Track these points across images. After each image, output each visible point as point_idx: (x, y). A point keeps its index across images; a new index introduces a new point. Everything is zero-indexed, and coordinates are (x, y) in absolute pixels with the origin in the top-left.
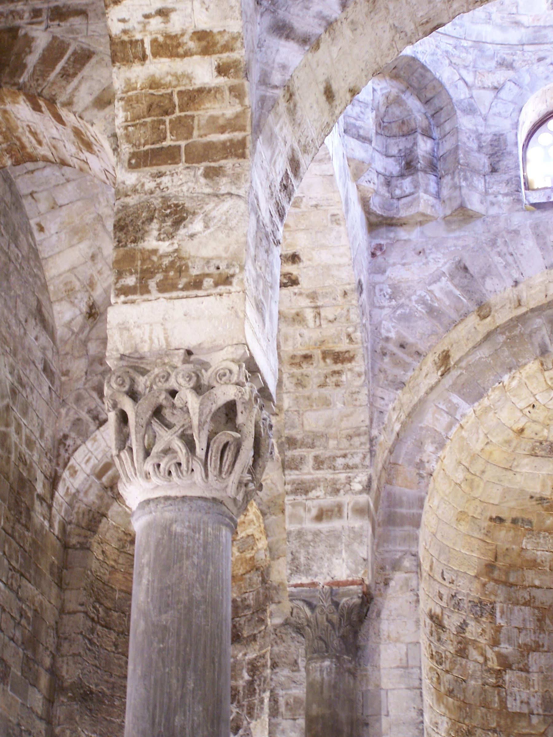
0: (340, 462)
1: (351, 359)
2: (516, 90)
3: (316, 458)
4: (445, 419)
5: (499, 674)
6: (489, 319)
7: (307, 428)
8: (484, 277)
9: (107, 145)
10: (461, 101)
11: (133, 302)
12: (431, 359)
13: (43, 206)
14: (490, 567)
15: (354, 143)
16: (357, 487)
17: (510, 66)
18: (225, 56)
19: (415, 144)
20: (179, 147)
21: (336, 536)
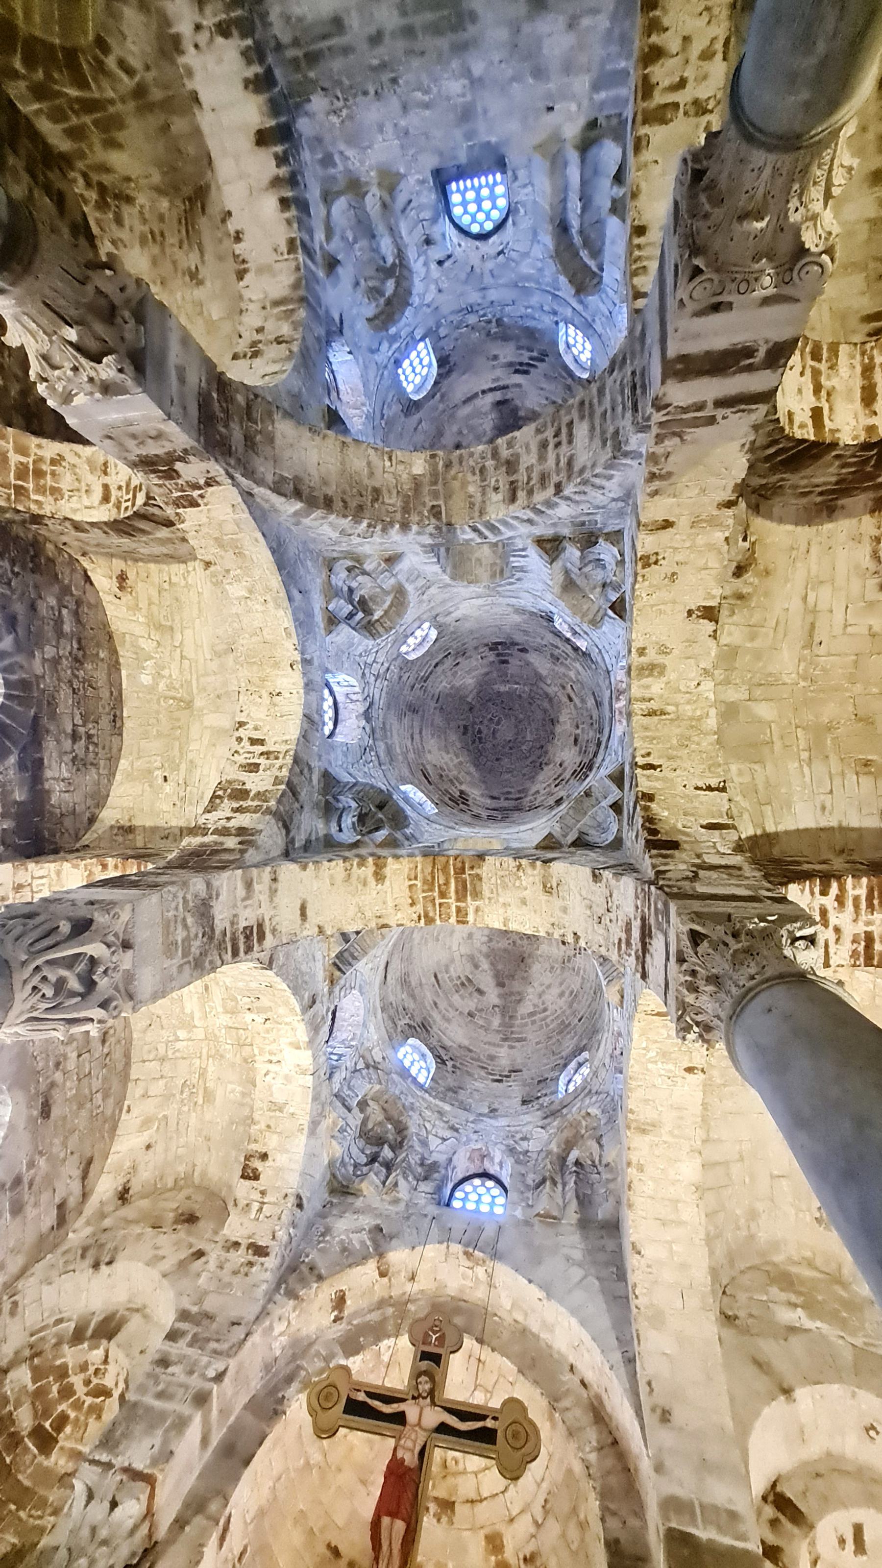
1: (267, 1255)
6: (386, 1279)
8: (391, 1238)
13: (139, 1092)
16: (211, 1373)
17: (457, 1130)
21: (162, 1416)
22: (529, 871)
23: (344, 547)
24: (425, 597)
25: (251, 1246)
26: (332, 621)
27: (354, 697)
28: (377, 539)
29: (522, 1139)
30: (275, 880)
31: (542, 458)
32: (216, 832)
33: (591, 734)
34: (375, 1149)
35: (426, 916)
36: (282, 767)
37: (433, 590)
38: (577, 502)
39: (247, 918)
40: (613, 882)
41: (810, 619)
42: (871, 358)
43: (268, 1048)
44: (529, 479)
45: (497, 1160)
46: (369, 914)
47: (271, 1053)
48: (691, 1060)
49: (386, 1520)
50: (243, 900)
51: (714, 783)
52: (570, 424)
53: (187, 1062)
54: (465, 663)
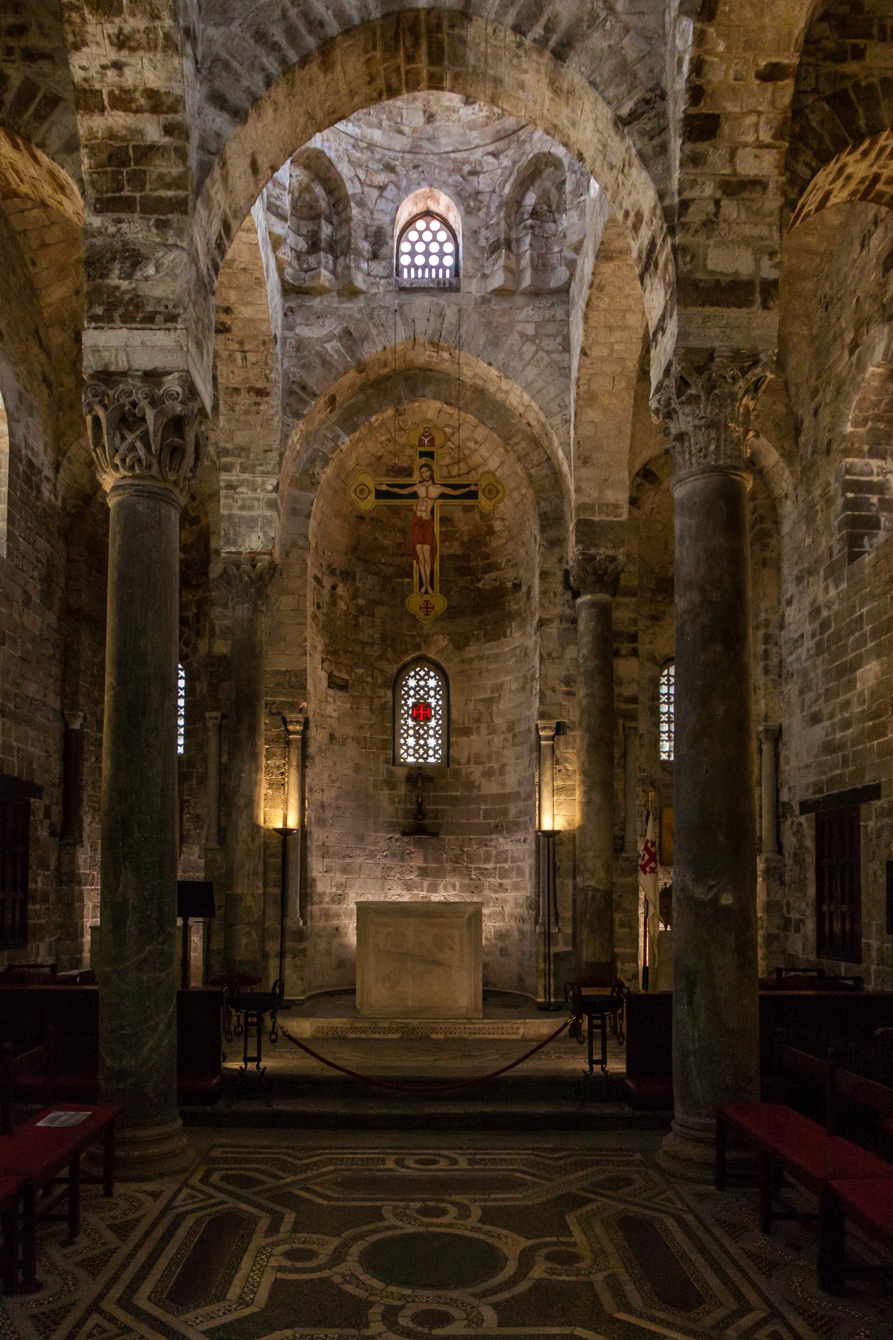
0: (259, 468)
1: (268, 394)
2: (395, 191)
3: (242, 464)
4: (331, 445)
5: (356, 617)
7: (236, 442)
9: (76, 188)
10: (354, 195)
11: (102, 328)
12: (322, 401)
14: (355, 549)
15: (273, 219)
16: (270, 488)
19: (320, 227)
20: (135, 198)
25: (250, 389)
34: (311, 226)
49: (419, 547)
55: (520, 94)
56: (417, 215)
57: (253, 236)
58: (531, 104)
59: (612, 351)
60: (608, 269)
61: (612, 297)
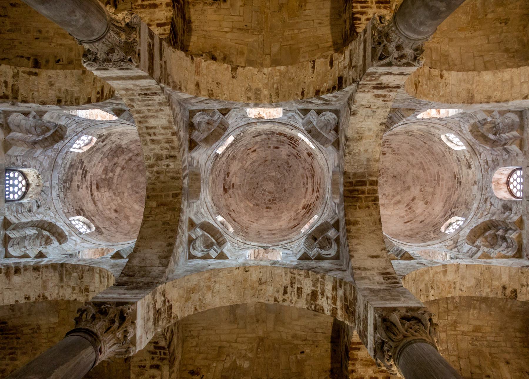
17: (486, 199)
18: (338, 284)
22: (351, 148)
23: (186, 246)
24: (206, 215)
26: (222, 256)
27: (256, 254)
28: (184, 228)
29: (487, 165)
30: (359, 268)
31: (158, 142)
32: (335, 303)
33: (274, 139)
34: (499, 239)
35: (374, 201)
36: (300, 276)
37: (202, 210)
38: (180, 126)
39: (379, 278)
40: (357, 104)
41: (235, 30)
42: (139, 5)
43: (447, 289)
44: (166, 149)
45: (499, 176)
46: (374, 228)
47: (450, 287)
48: (437, 76)
50: (370, 280)
51: (310, 65)
52: (147, 128)
53: (459, 342)
54: (233, 207)
55: (370, 151)
56: (508, 188)
57: (461, 266)
58: (372, 147)
59: (524, 82)
60: (477, 97)
61: (494, 91)
